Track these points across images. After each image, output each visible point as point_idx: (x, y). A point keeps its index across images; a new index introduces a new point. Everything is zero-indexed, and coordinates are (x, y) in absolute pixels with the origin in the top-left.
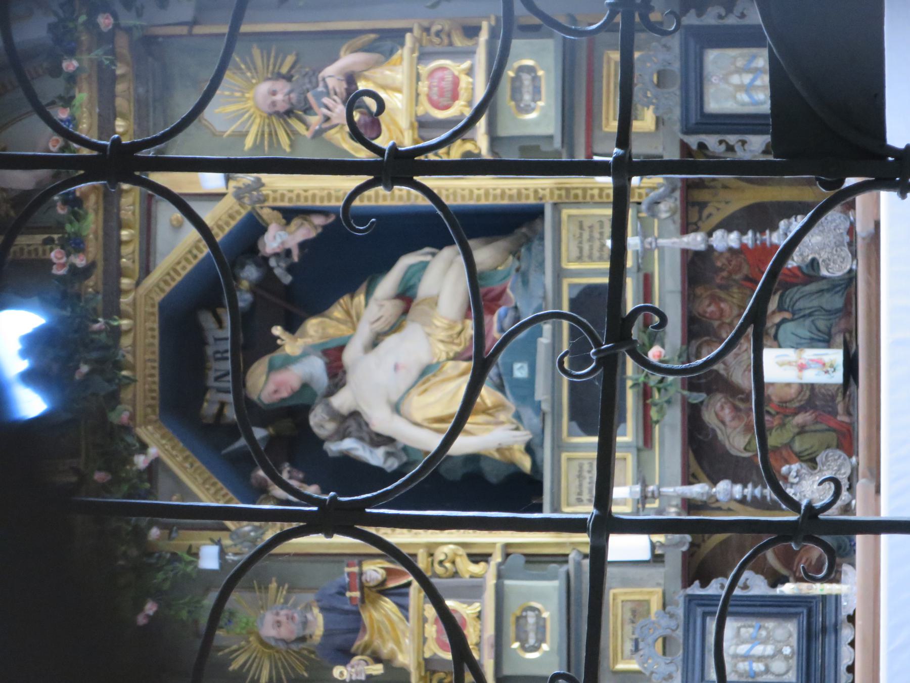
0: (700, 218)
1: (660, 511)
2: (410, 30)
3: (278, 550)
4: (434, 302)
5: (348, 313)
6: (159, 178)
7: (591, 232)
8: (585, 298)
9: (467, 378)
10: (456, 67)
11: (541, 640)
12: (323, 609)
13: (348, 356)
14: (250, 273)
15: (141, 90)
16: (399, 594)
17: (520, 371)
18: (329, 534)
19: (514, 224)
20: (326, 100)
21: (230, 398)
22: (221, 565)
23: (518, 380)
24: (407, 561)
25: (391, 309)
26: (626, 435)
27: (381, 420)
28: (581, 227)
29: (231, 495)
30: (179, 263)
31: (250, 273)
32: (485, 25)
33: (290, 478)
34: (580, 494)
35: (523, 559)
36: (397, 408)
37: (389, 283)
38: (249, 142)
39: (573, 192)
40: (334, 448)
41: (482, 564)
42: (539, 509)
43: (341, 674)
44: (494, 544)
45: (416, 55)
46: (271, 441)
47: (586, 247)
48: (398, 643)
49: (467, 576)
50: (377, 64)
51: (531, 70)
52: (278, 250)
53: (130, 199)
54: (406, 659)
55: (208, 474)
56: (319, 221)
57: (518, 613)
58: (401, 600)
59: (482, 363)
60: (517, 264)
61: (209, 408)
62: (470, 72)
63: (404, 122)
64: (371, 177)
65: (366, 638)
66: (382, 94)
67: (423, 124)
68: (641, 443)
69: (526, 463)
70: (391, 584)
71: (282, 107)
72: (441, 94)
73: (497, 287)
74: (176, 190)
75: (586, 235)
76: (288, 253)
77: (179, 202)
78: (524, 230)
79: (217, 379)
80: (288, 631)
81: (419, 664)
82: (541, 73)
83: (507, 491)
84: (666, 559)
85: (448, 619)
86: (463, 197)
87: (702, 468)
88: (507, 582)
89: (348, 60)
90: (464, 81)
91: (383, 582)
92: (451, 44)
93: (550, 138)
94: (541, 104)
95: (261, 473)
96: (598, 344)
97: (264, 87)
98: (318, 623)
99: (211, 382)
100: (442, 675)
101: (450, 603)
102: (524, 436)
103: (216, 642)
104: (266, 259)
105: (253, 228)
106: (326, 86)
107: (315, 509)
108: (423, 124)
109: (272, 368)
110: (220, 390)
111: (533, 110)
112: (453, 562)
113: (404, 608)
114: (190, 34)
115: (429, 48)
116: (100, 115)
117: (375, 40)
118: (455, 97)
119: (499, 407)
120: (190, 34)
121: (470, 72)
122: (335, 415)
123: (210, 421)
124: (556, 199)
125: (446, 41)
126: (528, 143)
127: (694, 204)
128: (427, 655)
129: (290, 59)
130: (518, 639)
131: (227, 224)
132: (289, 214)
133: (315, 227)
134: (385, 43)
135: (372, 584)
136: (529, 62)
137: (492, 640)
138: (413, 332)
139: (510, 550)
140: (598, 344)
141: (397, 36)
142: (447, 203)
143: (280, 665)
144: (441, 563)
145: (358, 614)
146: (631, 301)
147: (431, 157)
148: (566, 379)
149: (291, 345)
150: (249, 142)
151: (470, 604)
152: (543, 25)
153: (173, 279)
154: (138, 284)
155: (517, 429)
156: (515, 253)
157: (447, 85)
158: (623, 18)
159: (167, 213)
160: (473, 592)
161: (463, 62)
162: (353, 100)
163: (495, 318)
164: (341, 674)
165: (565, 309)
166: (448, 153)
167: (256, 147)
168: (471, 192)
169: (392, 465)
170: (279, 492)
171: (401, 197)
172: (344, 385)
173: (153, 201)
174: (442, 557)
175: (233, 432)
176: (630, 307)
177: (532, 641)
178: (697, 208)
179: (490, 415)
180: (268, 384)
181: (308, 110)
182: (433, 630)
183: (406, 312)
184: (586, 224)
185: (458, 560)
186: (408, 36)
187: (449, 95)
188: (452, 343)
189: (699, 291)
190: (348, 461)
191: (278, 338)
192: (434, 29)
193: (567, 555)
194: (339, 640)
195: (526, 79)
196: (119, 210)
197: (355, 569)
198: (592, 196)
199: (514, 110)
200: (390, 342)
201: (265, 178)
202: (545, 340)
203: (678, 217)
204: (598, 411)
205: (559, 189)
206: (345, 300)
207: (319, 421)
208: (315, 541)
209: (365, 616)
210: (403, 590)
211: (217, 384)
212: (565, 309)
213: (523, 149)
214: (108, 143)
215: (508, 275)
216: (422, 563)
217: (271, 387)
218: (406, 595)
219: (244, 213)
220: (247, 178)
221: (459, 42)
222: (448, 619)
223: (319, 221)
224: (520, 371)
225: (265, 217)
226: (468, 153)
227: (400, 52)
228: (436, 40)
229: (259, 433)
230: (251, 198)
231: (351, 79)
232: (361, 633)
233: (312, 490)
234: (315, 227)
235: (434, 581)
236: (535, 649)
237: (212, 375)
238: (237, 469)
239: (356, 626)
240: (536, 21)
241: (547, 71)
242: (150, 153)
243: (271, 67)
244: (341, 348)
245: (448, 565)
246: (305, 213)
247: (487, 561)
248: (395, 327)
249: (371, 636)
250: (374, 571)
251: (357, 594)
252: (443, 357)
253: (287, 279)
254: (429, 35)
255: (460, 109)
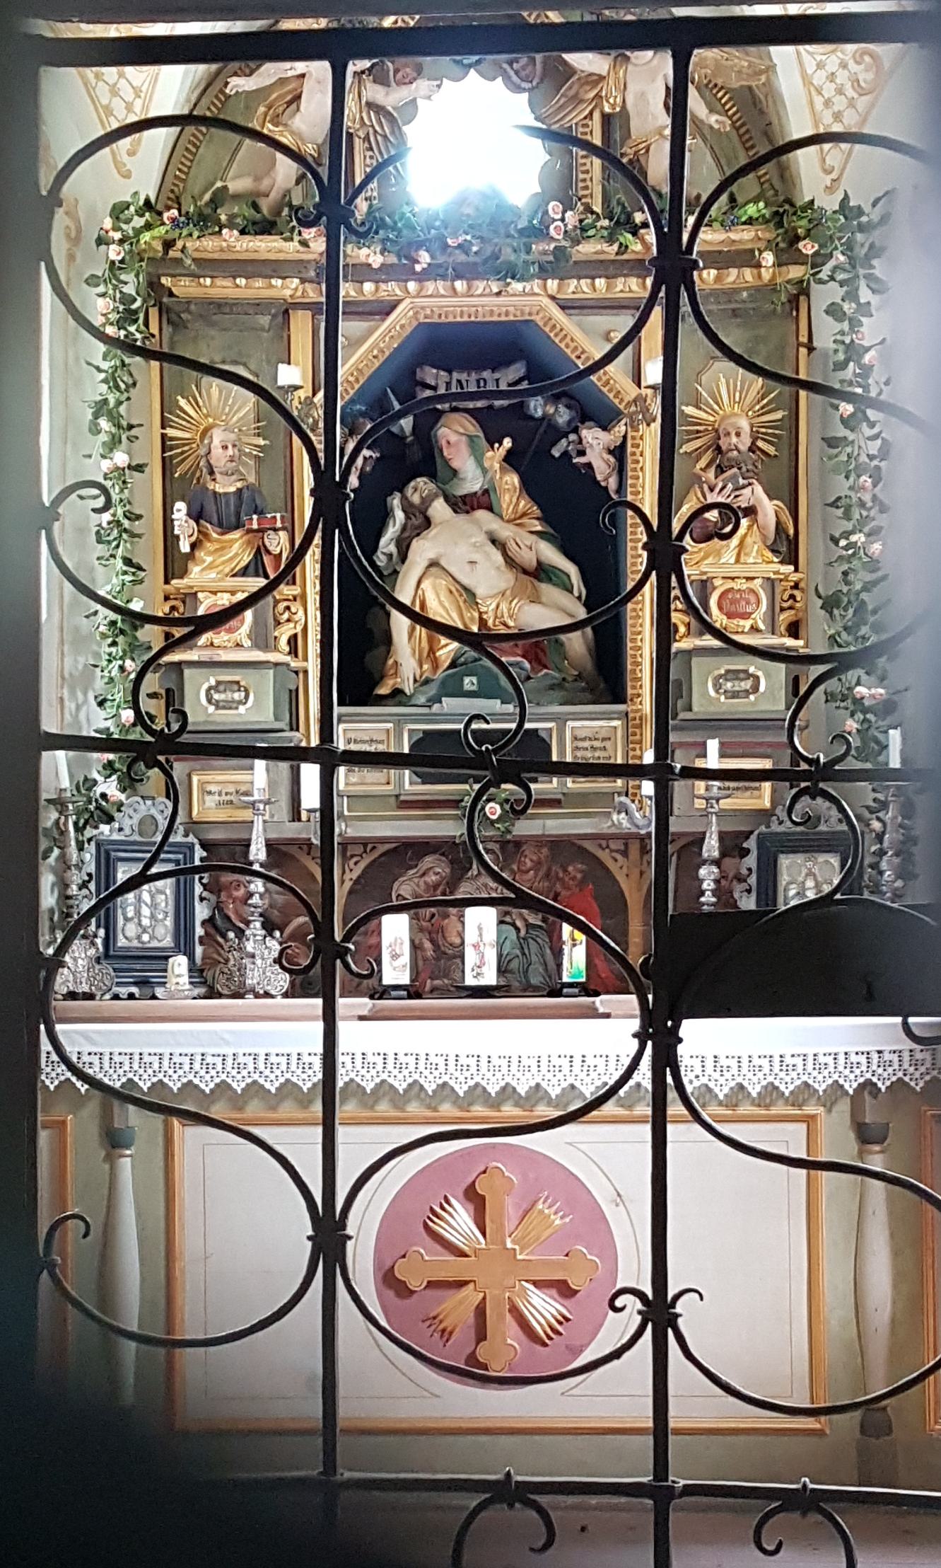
0: (612, 851)
1: (341, 815)
2: (796, 570)
3: (296, 440)
4: (536, 599)
5: (524, 515)
6: (657, 314)
7: (600, 749)
8: (537, 742)
9: (461, 626)
10: (759, 617)
11: (218, 705)
12: (240, 491)
13: (481, 514)
14: (563, 416)
15: (745, 294)
16: (255, 567)
17: (469, 683)
18: (313, 493)
19: (606, 680)
20: (730, 486)
21: (442, 391)
22: (282, 388)
23: (462, 681)
24: (288, 573)
25: (528, 558)
26: (407, 781)
27: (422, 550)
28: (604, 739)
29: (347, 398)
30: (572, 340)
31: (563, 416)
32: (801, 643)
33: (365, 458)
34: (355, 741)
35: (293, 687)
36: (434, 564)
37: (552, 555)
38: (689, 410)
39: (638, 731)
40: (396, 501)
41: (287, 649)
42: (339, 705)
43: (179, 510)
44: (306, 659)
45: (773, 576)
46: (401, 438)
47: (587, 744)
48: (210, 567)
49: (276, 634)
50: (764, 538)
51: (755, 689)
52: (584, 441)
53: (636, 287)
54: (196, 576)
55: (368, 373)
56: (612, 484)
57: (242, 683)
58: (251, 569)
59: (479, 641)
60: (570, 679)
61: (430, 374)
62: (755, 629)
63: (708, 568)
64: (655, 528)
65: (215, 535)
66: (735, 541)
67: (705, 586)
68: (402, 798)
69: (383, 690)
70: (266, 559)
71: (723, 443)
72: (733, 602)
73: (552, 657)
74: (643, 333)
75: (597, 744)
76: (582, 453)
77: (633, 334)
78: (602, 685)
79: (459, 381)
80: (219, 457)
81: (192, 587)
82: (752, 697)
83: (357, 669)
84: (296, 824)
85: (236, 610)
86: (634, 626)
87: (381, 856)
88: (271, 672)
89: (769, 509)
90: (747, 624)
91: (268, 552)
92: (782, 610)
93: (689, 708)
94: (723, 698)
95: (369, 426)
96: (495, 752)
97: (744, 424)
98: (224, 486)
99: (455, 375)
100: (181, 610)
101: (248, 615)
102: (408, 688)
103: (207, 380)
104: (576, 430)
105: (605, 416)
106: (744, 487)
107: (337, 479)
108: (705, 586)
109: (471, 438)
110: (448, 384)
111: (717, 692)
112: (288, 620)
113: (244, 572)
114: (799, 345)
115: (778, 590)
116: (720, 252)
117: (788, 536)
118: (730, 616)
119: (435, 664)
120: (799, 345)
121: (755, 629)
122: (427, 502)
123: (419, 375)
124: (631, 715)
125: (785, 605)
126: (684, 688)
127: (626, 845)
128: (200, 595)
129: (771, 450)
130: (219, 683)
131: (610, 391)
132: (619, 452)
133: (606, 479)
134: (786, 546)
135: (266, 540)
136: (762, 688)
137: (216, 659)
138: (506, 579)
139: (301, 675)
140: (495, 752)
141: (792, 558)
142: (630, 606)
143: (186, 448)
144: (288, 608)
145: (237, 527)
146: (544, 786)
147: (676, 592)
148: (461, 726)
149: (494, 457)
150: (689, 410)
151: (249, 637)
152: (799, 697)
153: (556, 335)
154: (553, 298)
155: (415, 681)
156: (579, 677)
157: (742, 607)
158: (804, 771)
159: (625, 322)
160: (262, 639)
161: (764, 622)
162: (731, 514)
163: (519, 659)
164: (179, 510)
165: (527, 726)
166: (676, 610)
167: (687, 419)
168: (639, 633)
169: (381, 560)
170: (351, 446)
171: (636, 558)
172: (456, 512)
173: (633, 311)
174: (293, 610)
175: (406, 397)
176: (533, 786)
177: (216, 696)
178: (622, 848)
179: (428, 655)
180: (455, 436)
181: (720, 470)
182: (225, 600)
183: (525, 572)
184: (608, 744)
185: (292, 625)
186: (792, 568)
187: (733, 609)
188: (496, 617)
189: (545, 851)
190: (385, 515)
191: (501, 444)
192: (796, 592)
193: (298, 730)
194: (211, 508)
195: (747, 685)
196: (625, 276)
197: (279, 525)
198: (634, 749)
199: (716, 673)
200: (498, 557)
201: (656, 426)
202: (496, 705)
203: (613, 830)
204: (432, 756)
205: (641, 719)
206: (536, 510)
207: (420, 487)
208: (306, 479)
209: (236, 535)
210: (261, 571)
211: (454, 383)
212: (527, 726)
213: (679, 684)
214: (694, 256)
215: (560, 671)
216: (285, 590)
217: (453, 438)
218: (257, 575)
219: (621, 407)
220: (656, 408)
221: (784, 618)
222: (236, 610)
223: (612, 484)
224: (469, 683)
225: (617, 429)
226: (676, 631)
227: (776, 560)
228: (786, 597)
229: (407, 423)
230: (636, 413)
231: (750, 511)
232: (219, 530)
233: (354, 481)
234: (606, 479)
235: (270, 599)
236: (209, 701)
237: (463, 377)
238: (375, 403)
239: (226, 527)
240: (803, 689)
241: (753, 704)
242: (685, 307)
243: (763, 430)
244: (490, 508)
245: (286, 616)
246: (621, 470)
247: (290, 653)
248: (510, 562)
249: (217, 541)
250: (279, 543)
251: (255, 526)
252: (483, 609)
253: (556, 453)
254: (792, 588)
255: (717, 618)
